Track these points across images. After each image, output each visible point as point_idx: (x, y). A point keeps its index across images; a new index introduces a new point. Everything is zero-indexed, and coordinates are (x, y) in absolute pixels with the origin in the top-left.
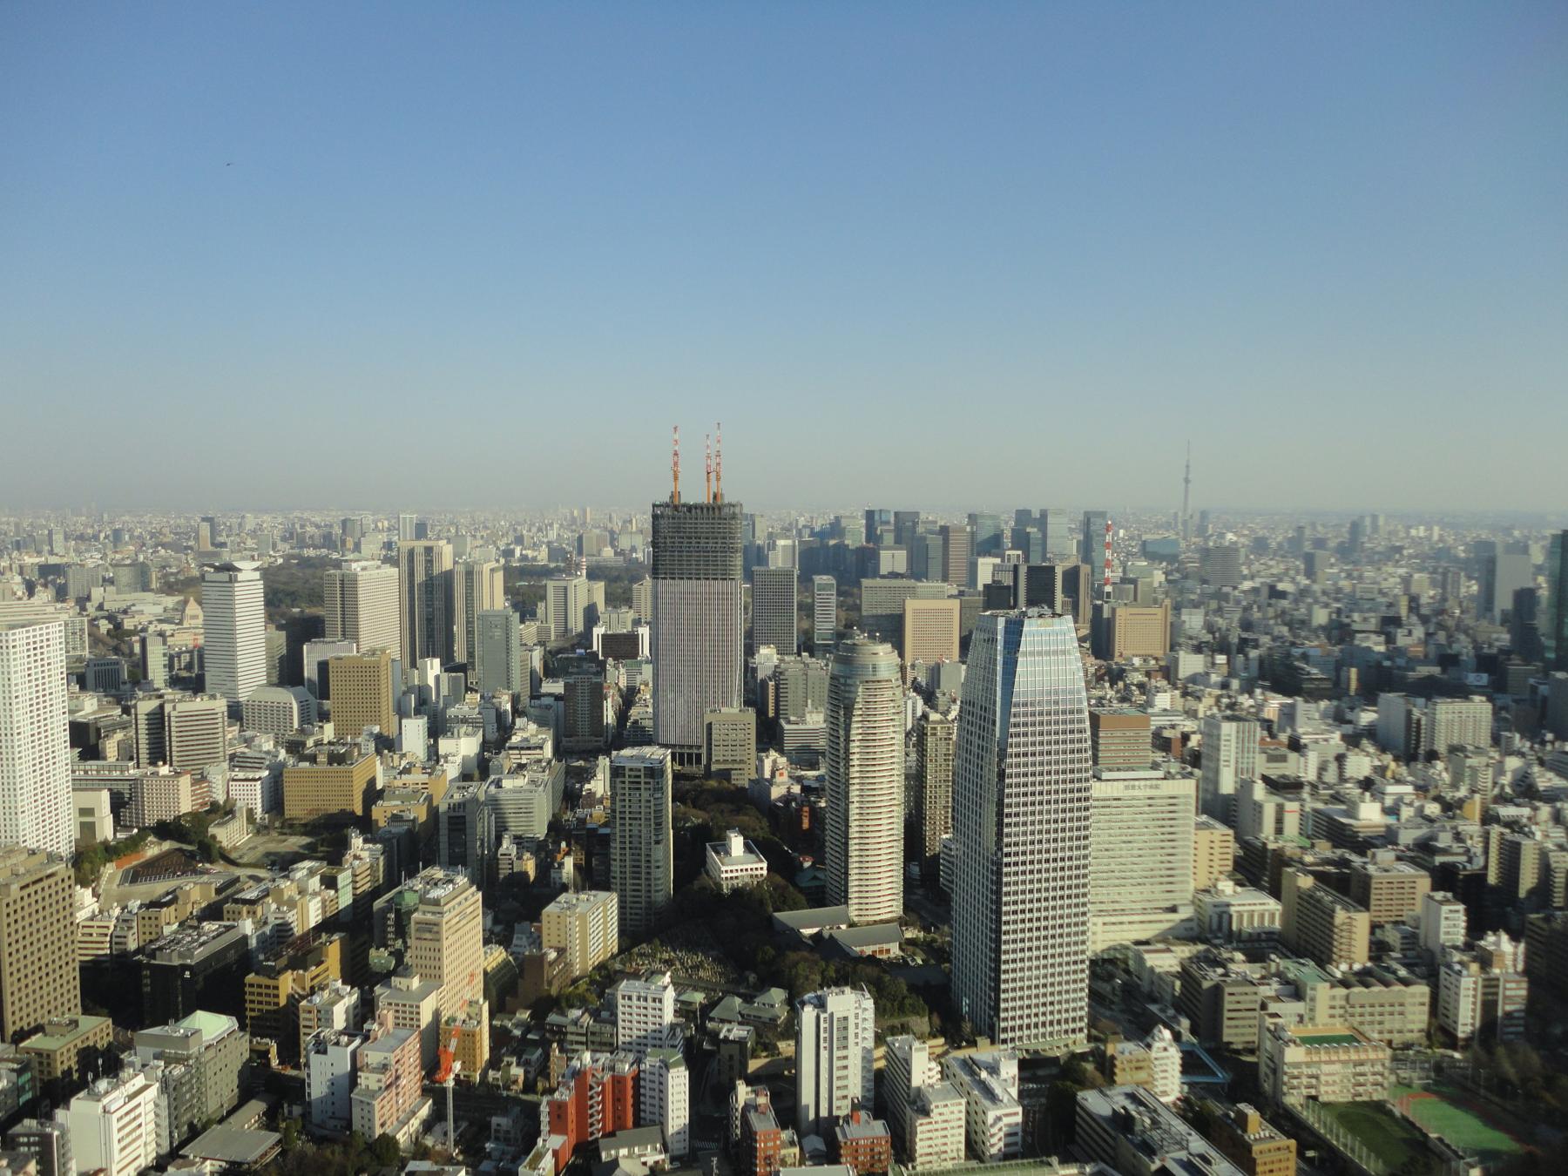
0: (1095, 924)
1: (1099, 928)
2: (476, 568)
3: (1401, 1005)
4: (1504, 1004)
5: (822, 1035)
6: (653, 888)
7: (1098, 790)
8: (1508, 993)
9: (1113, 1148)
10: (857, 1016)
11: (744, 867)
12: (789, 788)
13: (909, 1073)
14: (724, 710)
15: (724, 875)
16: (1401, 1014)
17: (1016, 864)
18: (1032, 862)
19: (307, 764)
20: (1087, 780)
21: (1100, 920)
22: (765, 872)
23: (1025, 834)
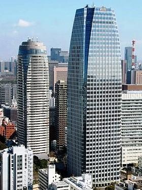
1: (126, 150)
5: (11, 163)
7: (124, 96)
12: (4, 120)
13: (48, 178)
17: (91, 117)
18: (98, 117)
20: (119, 92)
23: (95, 97)
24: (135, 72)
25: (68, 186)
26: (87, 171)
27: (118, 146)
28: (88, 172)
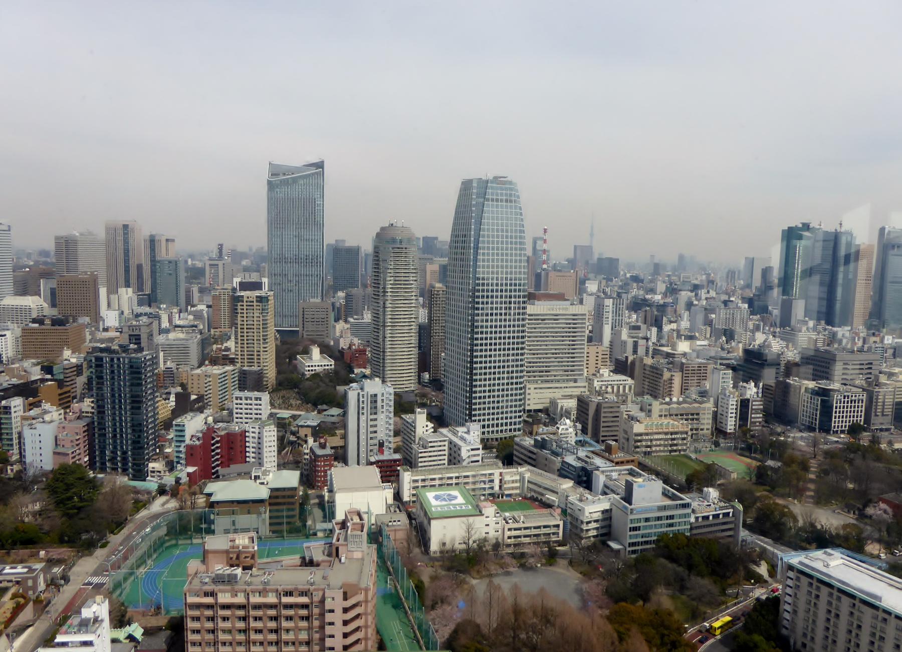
0: (529, 389)
1: (532, 389)
2: (157, 238)
3: (698, 414)
4: (752, 414)
6: (261, 357)
7: (531, 309)
8: (754, 407)
9: (534, 460)
10: (383, 395)
11: (320, 364)
13: (415, 428)
14: (312, 300)
15: (307, 369)
16: (697, 419)
19: (36, 325)
21: (532, 386)
22: (333, 367)
24: (547, 274)
25: (445, 441)
26: (473, 418)
27: (521, 383)
28: (475, 421)
